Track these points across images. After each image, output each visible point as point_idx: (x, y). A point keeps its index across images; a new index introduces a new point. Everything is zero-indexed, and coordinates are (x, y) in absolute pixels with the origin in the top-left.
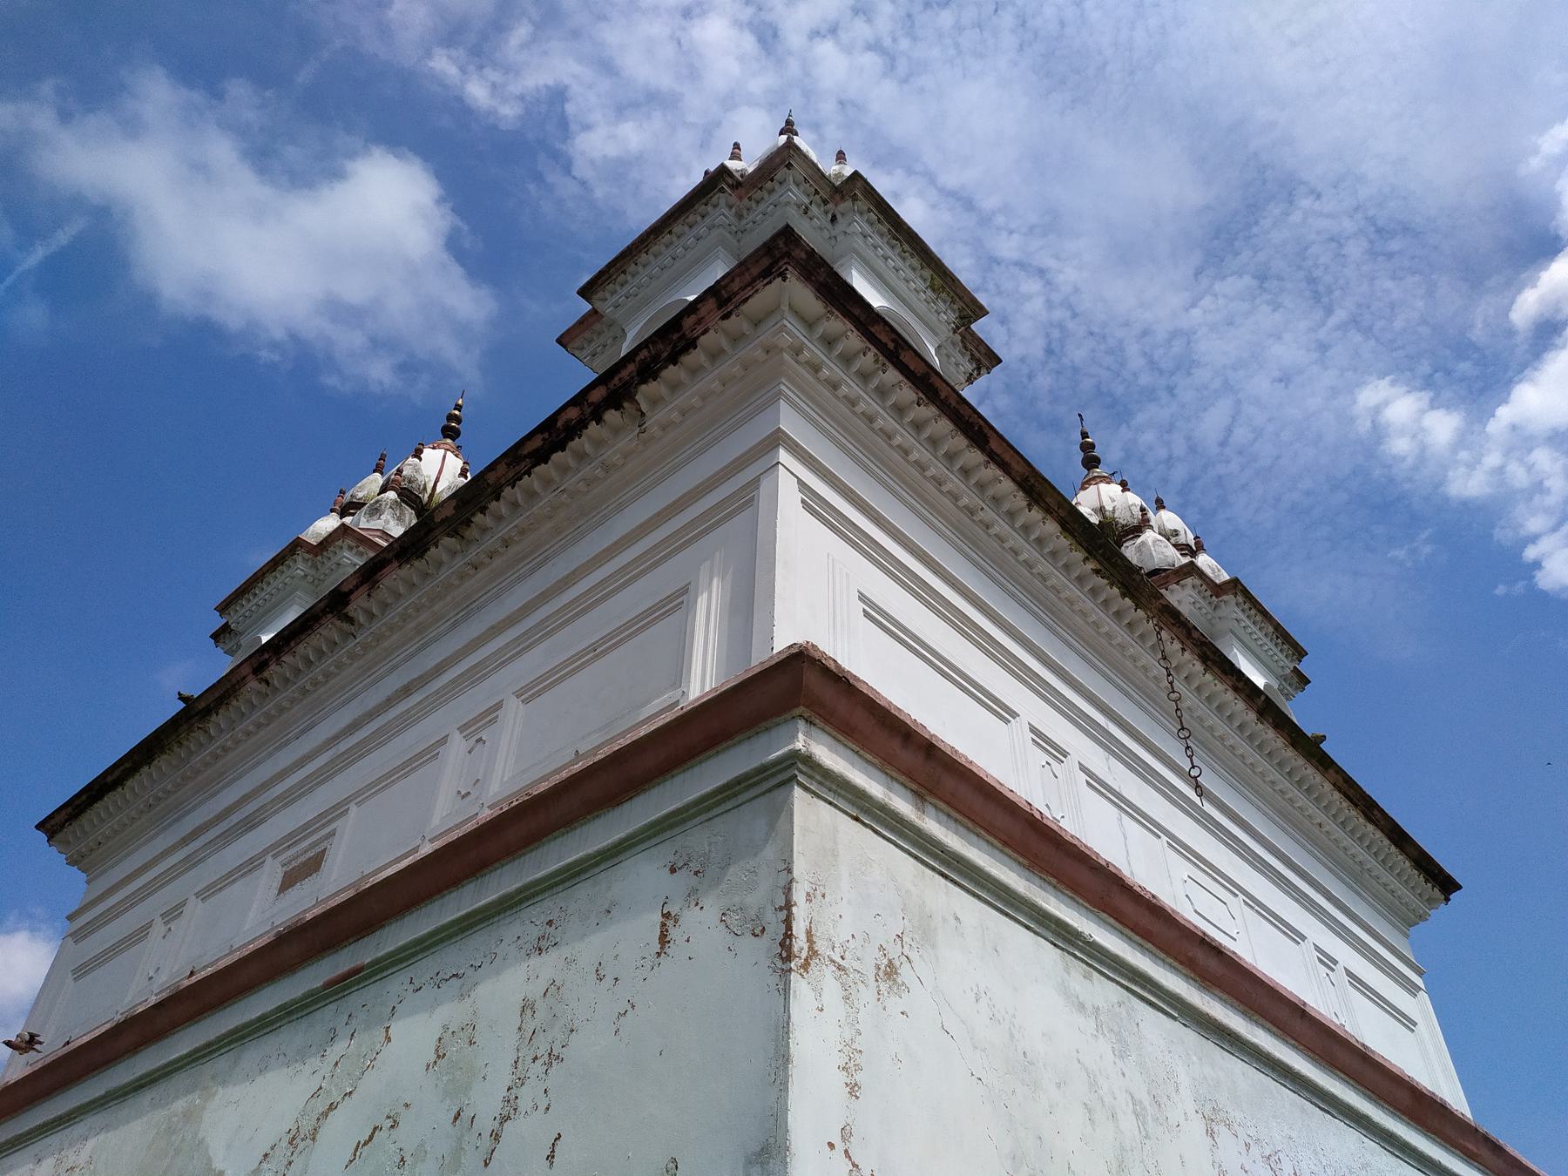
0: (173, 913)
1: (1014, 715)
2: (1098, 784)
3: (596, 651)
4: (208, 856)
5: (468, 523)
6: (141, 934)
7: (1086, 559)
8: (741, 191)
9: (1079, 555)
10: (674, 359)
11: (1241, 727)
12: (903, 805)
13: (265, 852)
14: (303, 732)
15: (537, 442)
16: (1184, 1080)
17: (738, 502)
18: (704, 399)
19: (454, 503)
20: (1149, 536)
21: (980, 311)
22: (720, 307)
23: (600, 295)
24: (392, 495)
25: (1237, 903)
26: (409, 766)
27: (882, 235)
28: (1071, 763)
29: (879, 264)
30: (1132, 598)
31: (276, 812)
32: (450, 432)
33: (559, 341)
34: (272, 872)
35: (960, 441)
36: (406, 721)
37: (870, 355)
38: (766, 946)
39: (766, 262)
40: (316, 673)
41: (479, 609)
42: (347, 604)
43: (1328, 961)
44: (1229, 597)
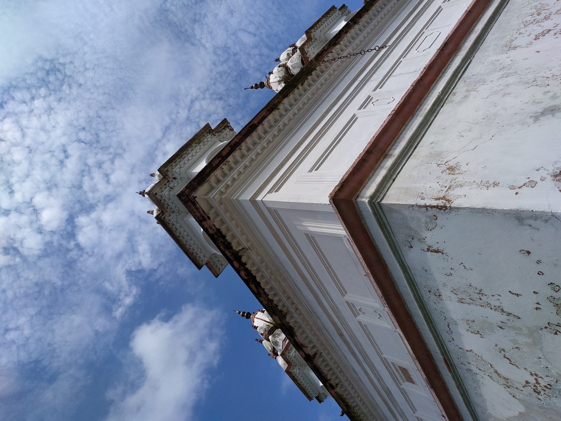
1: (354, 115)
2: (381, 85)
3: (328, 267)
4: (400, 408)
5: (281, 311)
7: (297, 88)
8: (164, 211)
9: (296, 91)
10: (224, 237)
11: (360, 30)
12: (389, 163)
13: (399, 388)
14: (355, 372)
15: (253, 286)
17: (275, 215)
18: (238, 227)
19: (274, 316)
20: (289, 64)
21: (208, 126)
22: (206, 220)
23: (200, 262)
24: (270, 337)
25: (427, 32)
27: (180, 161)
28: (372, 94)
30: (312, 71)
31: (384, 383)
32: (248, 316)
33: (217, 277)
34: (406, 385)
35: (254, 134)
37: (223, 167)
38: (441, 216)
39: (190, 204)
40: (334, 367)
41: (312, 308)
42: (309, 355)
44: (312, 35)
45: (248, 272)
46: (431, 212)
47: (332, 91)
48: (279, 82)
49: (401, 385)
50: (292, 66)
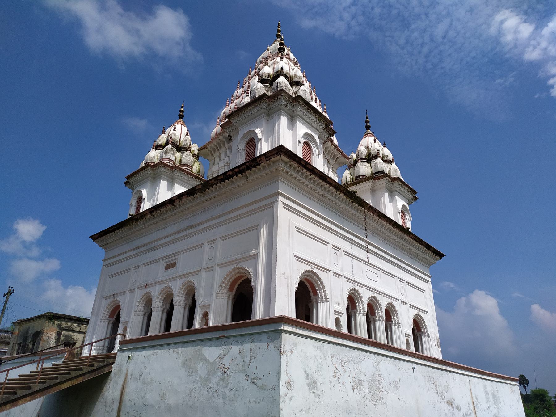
0: (136, 267)
1: (328, 243)
2: (347, 253)
3: (239, 233)
5: (205, 191)
6: (128, 270)
9: (348, 199)
10: (255, 167)
13: (160, 259)
15: (222, 177)
16: (329, 352)
17: (269, 206)
20: (379, 160)
24: (170, 146)
25: (379, 273)
26: (195, 247)
27: (305, 109)
29: (304, 117)
32: (181, 117)
35: (320, 181)
36: (191, 235)
38: (278, 352)
39: (276, 151)
40: (167, 215)
43: (402, 280)
45: (231, 176)
46: (279, 349)
47: (347, 220)
48: (367, 148)
50: (376, 163)
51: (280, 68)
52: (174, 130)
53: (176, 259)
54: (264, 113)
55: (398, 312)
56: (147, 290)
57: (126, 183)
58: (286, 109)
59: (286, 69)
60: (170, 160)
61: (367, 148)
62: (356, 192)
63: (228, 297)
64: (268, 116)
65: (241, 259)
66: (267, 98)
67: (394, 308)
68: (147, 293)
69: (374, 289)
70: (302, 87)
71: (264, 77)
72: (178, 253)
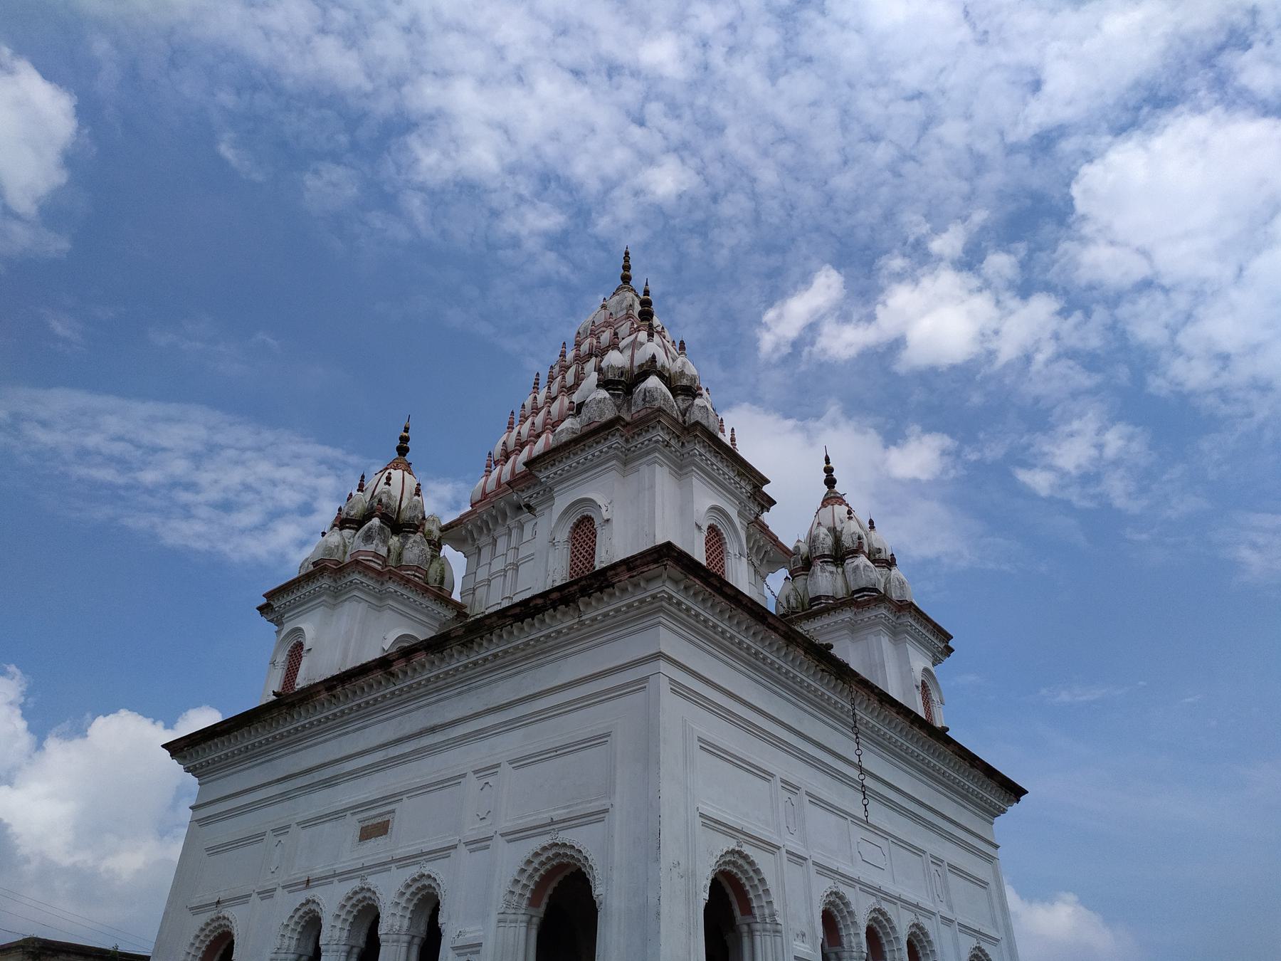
0: (282, 830)
5: (472, 642)
10: (601, 590)
13: (346, 810)
15: (517, 610)
20: (862, 560)
24: (376, 521)
34: (352, 825)
39: (655, 556)
43: (937, 861)
45: (540, 610)
48: (833, 530)
49: (353, 814)
51: (648, 356)
52: (388, 483)
53: (389, 812)
54: (616, 457)
55: (936, 947)
56: (308, 894)
57: (262, 609)
58: (666, 451)
59: (662, 358)
60: (377, 555)
61: (833, 530)
62: (832, 647)
63: (529, 923)
64: (625, 464)
65: (564, 821)
66: (624, 427)
67: (925, 934)
68: (308, 902)
69: (879, 890)
70: (698, 401)
71: (610, 376)
72: (395, 797)
